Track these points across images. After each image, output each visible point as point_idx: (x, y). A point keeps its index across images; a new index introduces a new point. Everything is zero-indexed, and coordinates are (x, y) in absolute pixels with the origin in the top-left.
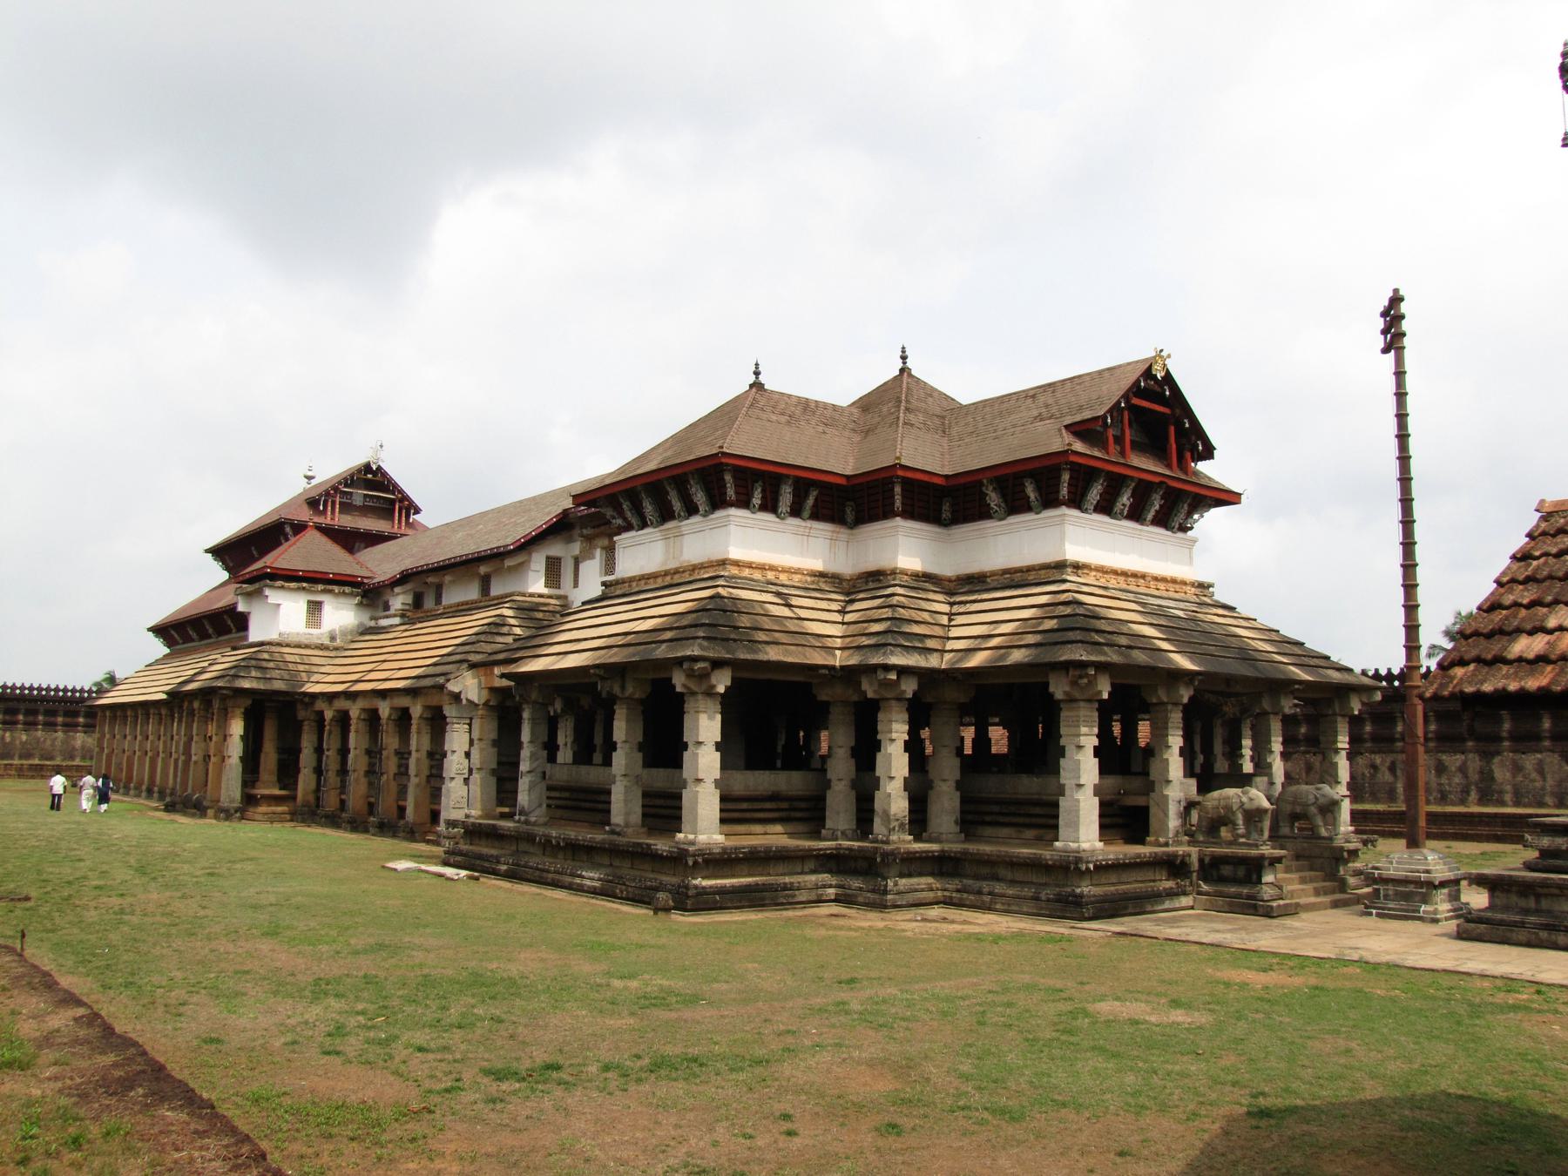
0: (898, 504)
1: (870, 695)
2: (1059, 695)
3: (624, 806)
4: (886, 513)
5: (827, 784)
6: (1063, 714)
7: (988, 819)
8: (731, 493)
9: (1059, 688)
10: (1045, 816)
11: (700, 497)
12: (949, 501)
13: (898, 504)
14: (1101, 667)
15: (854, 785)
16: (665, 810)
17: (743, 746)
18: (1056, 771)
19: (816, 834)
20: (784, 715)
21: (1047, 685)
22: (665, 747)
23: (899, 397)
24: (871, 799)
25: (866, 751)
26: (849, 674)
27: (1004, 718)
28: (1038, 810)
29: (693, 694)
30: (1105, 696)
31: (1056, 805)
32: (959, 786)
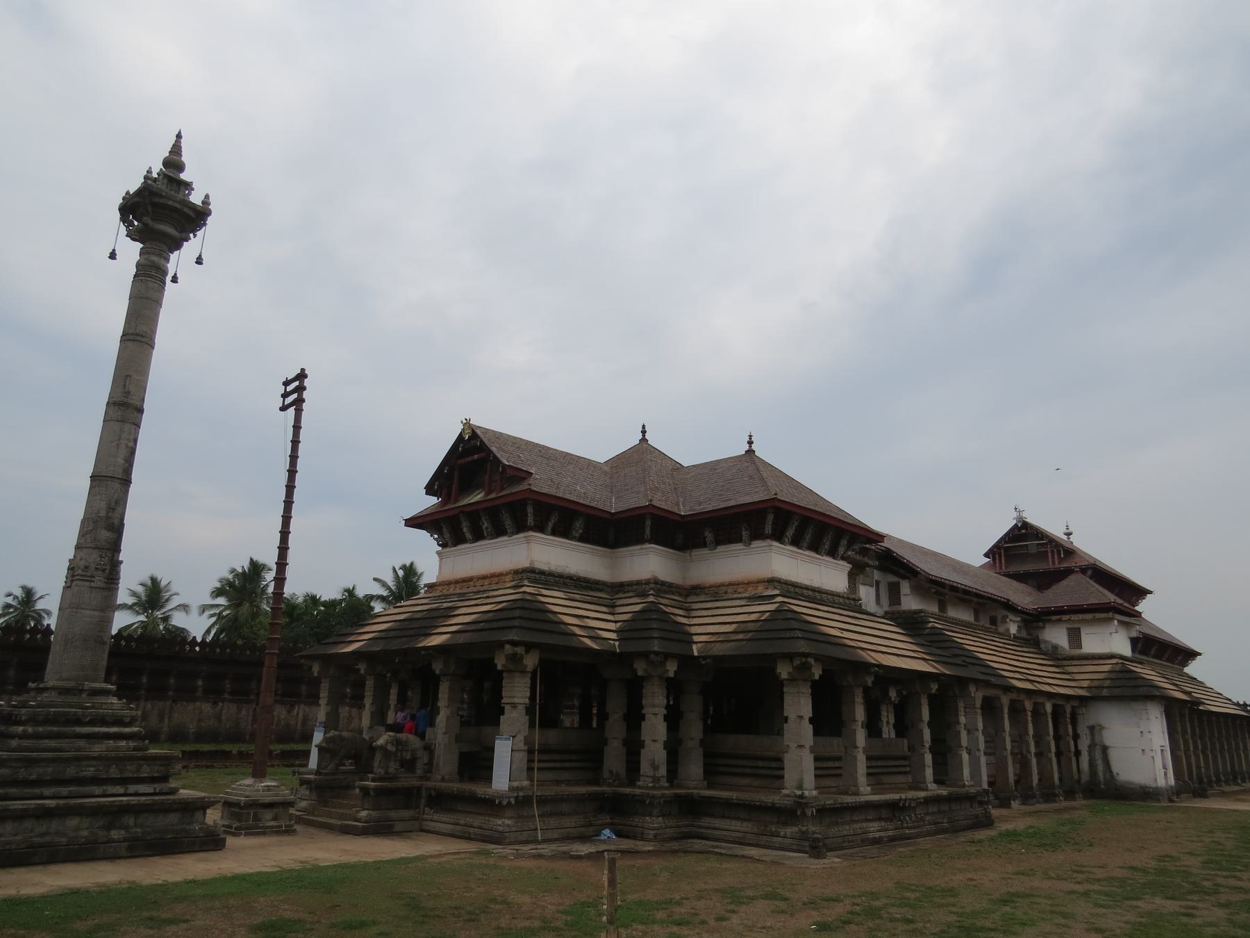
0: (648, 531)
1: (640, 673)
2: (784, 675)
3: (446, 761)
4: (639, 540)
5: (605, 742)
6: (785, 689)
7: (722, 769)
9: (784, 671)
10: (772, 769)
12: (684, 532)
13: (648, 531)
14: (818, 658)
15: (626, 743)
16: (477, 763)
17: (544, 714)
18: (780, 733)
19: (596, 782)
20: (579, 687)
21: (774, 669)
22: (484, 712)
23: (643, 455)
24: (639, 754)
25: (634, 718)
26: (622, 659)
27: (737, 693)
28: (760, 764)
29: (510, 671)
30: (817, 677)
31: (780, 760)
32: (702, 743)
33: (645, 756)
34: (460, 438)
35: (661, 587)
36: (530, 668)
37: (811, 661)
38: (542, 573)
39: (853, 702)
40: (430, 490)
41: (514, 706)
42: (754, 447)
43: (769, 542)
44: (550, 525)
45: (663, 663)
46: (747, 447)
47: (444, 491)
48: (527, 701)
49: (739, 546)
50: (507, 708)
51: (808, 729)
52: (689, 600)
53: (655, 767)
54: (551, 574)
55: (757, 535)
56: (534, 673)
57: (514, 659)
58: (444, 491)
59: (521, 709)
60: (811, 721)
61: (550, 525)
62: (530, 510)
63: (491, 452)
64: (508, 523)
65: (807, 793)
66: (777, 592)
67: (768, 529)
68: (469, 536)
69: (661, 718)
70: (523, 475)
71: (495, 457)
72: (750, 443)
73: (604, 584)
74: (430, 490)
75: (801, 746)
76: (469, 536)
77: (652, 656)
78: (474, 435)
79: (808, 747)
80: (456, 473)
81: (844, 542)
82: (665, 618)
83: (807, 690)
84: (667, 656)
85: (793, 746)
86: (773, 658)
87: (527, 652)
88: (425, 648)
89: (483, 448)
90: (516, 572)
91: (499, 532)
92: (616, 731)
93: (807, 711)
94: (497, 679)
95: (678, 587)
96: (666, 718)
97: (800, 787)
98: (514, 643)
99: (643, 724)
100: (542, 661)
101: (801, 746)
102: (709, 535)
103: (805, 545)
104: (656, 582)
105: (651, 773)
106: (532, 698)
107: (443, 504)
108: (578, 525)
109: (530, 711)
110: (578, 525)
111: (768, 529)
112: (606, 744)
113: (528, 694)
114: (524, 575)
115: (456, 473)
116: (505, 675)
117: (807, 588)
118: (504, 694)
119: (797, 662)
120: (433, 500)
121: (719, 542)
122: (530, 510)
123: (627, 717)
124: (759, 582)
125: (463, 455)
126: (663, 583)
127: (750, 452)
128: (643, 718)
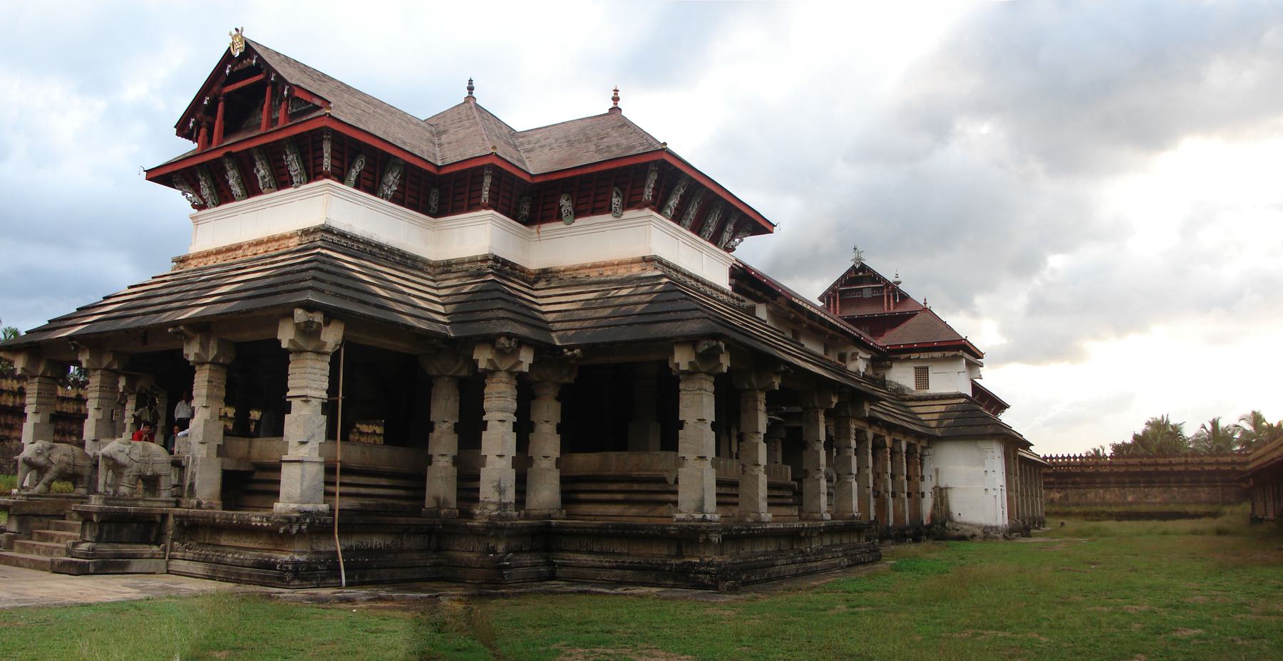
3: (206, 484)
7: (582, 496)
8: (327, 163)
11: (294, 167)
16: (248, 483)
33: (486, 474)
34: (228, 57)
35: (503, 267)
36: (330, 348)
37: (722, 345)
38: (343, 235)
39: (756, 410)
40: (183, 129)
41: (306, 399)
42: (620, 105)
43: (647, 211)
44: (354, 173)
45: (514, 352)
46: (611, 105)
47: (203, 131)
48: (325, 395)
49: (608, 217)
50: (296, 403)
51: (710, 438)
52: (536, 286)
53: (501, 490)
54: (354, 239)
55: (632, 202)
56: (335, 358)
57: (309, 331)
58: (203, 131)
59: (316, 405)
60: (714, 426)
61: (354, 173)
62: (327, 148)
63: (270, 70)
64: (294, 167)
65: (708, 516)
66: (658, 273)
67: (648, 194)
68: (237, 190)
69: (509, 427)
70: (318, 102)
71: (279, 76)
72: (616, 99)
73: (425, 262)
74: (183, 129)
75: (702, 458)
76: (237, 190)
77: (503, 340)
78: (249, 50)
79: (710, 459)
80: (221, 106)
81: (730, 227)
82: (512, 298)
83: (709, 386)
84: (522, 342)
85: (691, 457)
86: (668, 344)
87: (327, 323)
88: (175, 324)
89: (262, 67)
90: (306, 232)
91: (282, 181)
92: (443, 443)
93: (710, 414)
94: (279, 361)
95: (523, 270)
96: (516, 427)
97: (700, 509)
98: (309, 307)
99: (485, 435)
100: (346, 342)
101: (702, 458)
102: (566, 204)
103: (688, 223)
104: (496, 259)
105: (495, 497)
106: (332, 390)
107: (202, 147)
108: (392, 179)
109: (328, 408)
110: (392, 179)
111: (648, 194)
112: (430, 463)
113: (326, 385)
114: (318, 237)
115: (221, 106)
116: (291, 357)
117: (690, 276)
118: (290, 383)
119: (703, 347)
120: (188, 146)
121: (578, 214)
122: (327, 148)
123: (457, 428)
124: (633, 262)
125: (234, 77)
126: (505, 262)
127: (615, 110)
128: (484, 425)
